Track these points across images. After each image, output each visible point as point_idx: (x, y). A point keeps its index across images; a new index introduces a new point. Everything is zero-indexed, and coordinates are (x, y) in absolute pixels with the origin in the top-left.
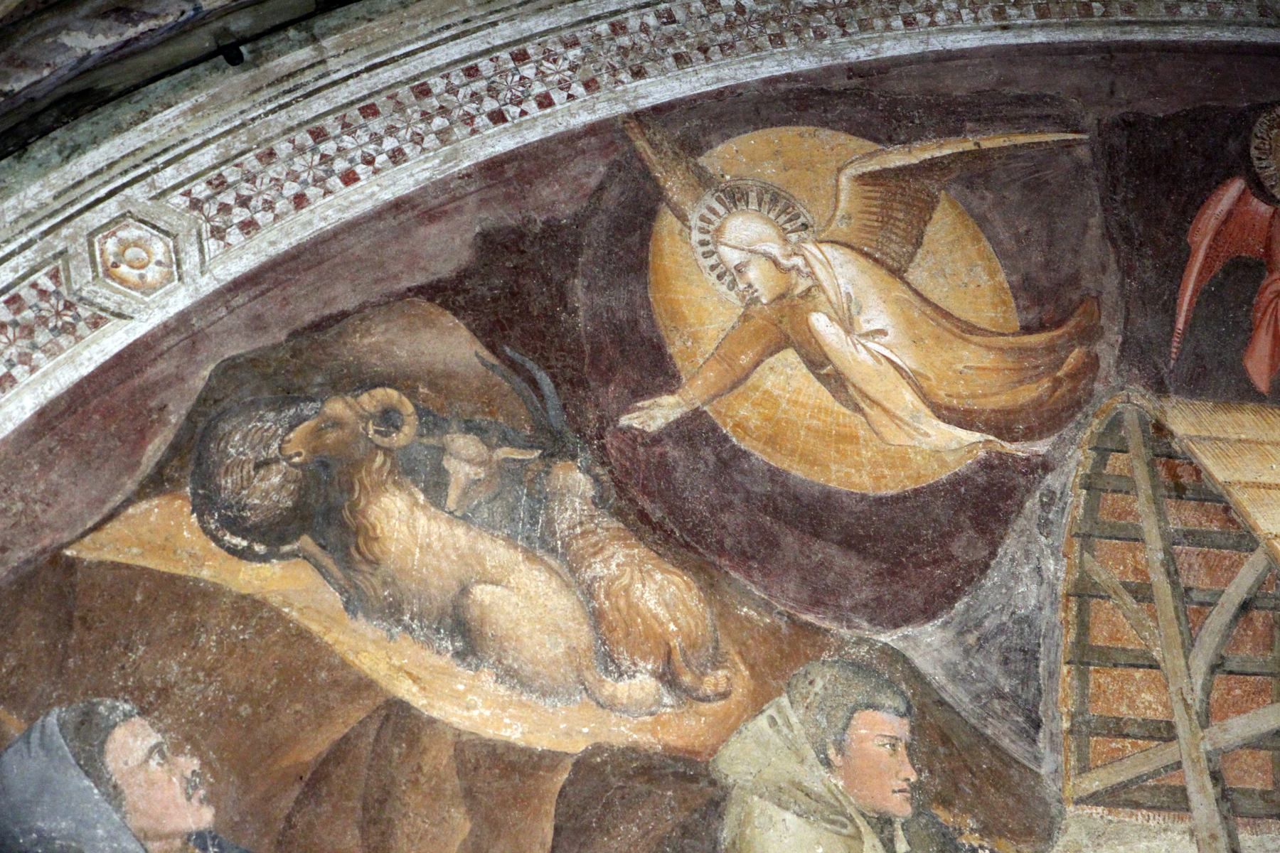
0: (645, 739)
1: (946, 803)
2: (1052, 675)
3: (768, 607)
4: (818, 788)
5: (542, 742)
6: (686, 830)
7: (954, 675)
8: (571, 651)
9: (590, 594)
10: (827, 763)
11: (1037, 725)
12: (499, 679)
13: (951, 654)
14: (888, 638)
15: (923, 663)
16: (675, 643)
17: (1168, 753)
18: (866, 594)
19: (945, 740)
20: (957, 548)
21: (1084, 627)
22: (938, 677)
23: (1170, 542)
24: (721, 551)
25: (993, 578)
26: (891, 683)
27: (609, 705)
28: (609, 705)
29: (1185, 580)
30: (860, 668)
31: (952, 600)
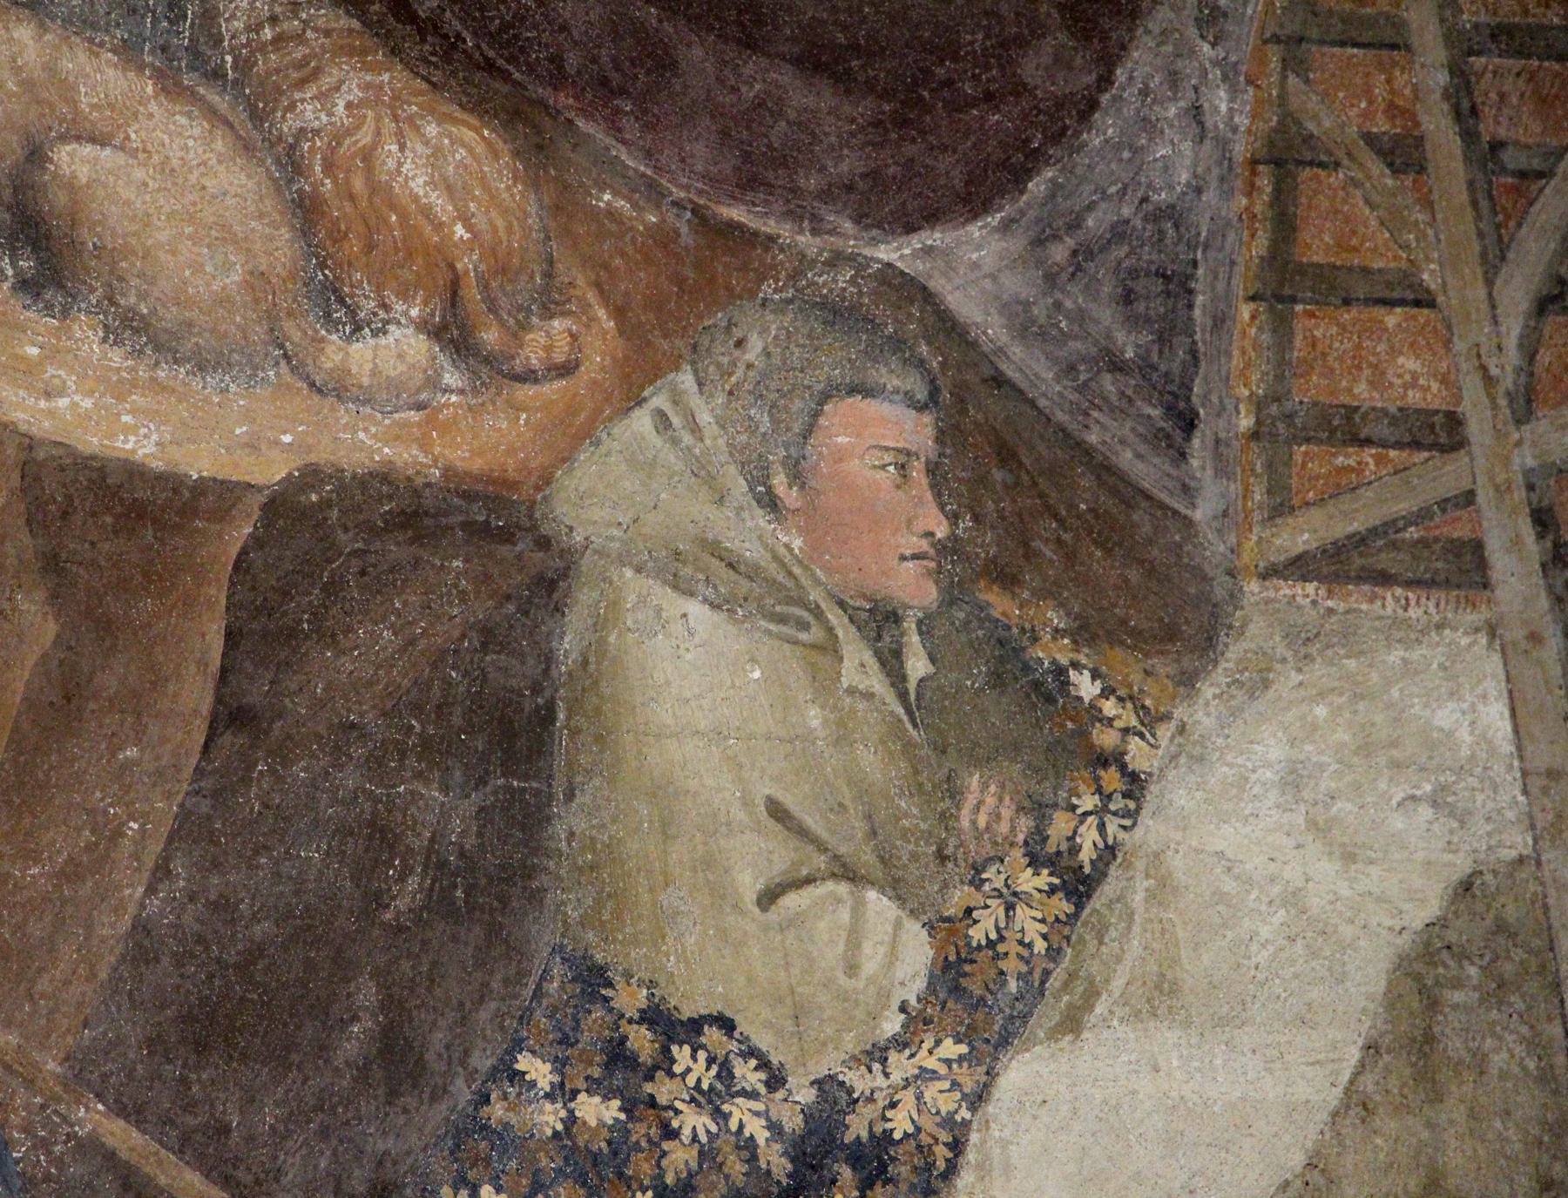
0: (406, 456)
1: (1007, 580)
2: (1220, 321)
3: (653, 192)
4: (752, 551)
5: (200, 463)
6: (489, 637)
7: (1025, 327)
8: (257, 281)
9: (292, 163)
10: (770, 503)
11: (1189, 423)
12: (112, 336)
13: (1016, 284)
14: (892, 252)
15: (964, 303)
16: (467, 263)
17: (1448, 475)
18: (849, 165)
19: (1006, 455)
20: (1032, 68)
21: (1285, 225)
22: (991, 328)
23: (1462, 47)
24: (558, 77)
25: (1106, 128)
26: (898, 344)
27: (337, 389)
28: (337, 389)
29: (1487, 129)
30: (837, 313)
31: (1020, 176)
